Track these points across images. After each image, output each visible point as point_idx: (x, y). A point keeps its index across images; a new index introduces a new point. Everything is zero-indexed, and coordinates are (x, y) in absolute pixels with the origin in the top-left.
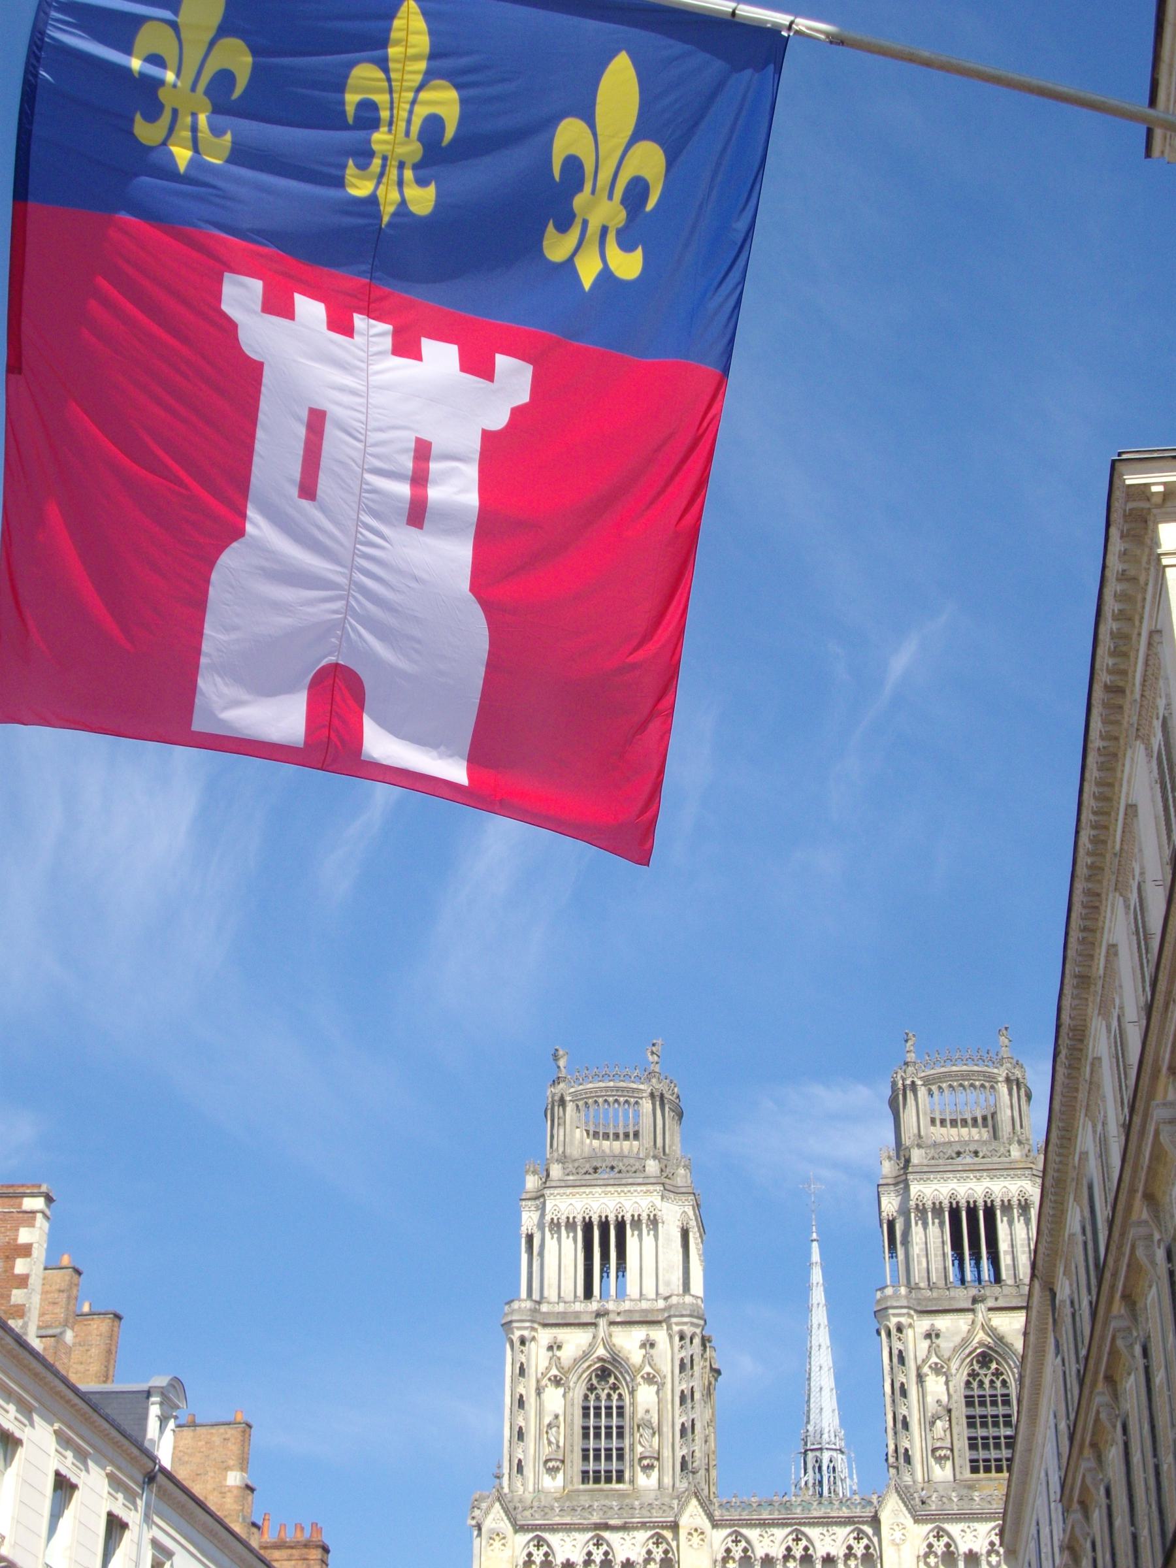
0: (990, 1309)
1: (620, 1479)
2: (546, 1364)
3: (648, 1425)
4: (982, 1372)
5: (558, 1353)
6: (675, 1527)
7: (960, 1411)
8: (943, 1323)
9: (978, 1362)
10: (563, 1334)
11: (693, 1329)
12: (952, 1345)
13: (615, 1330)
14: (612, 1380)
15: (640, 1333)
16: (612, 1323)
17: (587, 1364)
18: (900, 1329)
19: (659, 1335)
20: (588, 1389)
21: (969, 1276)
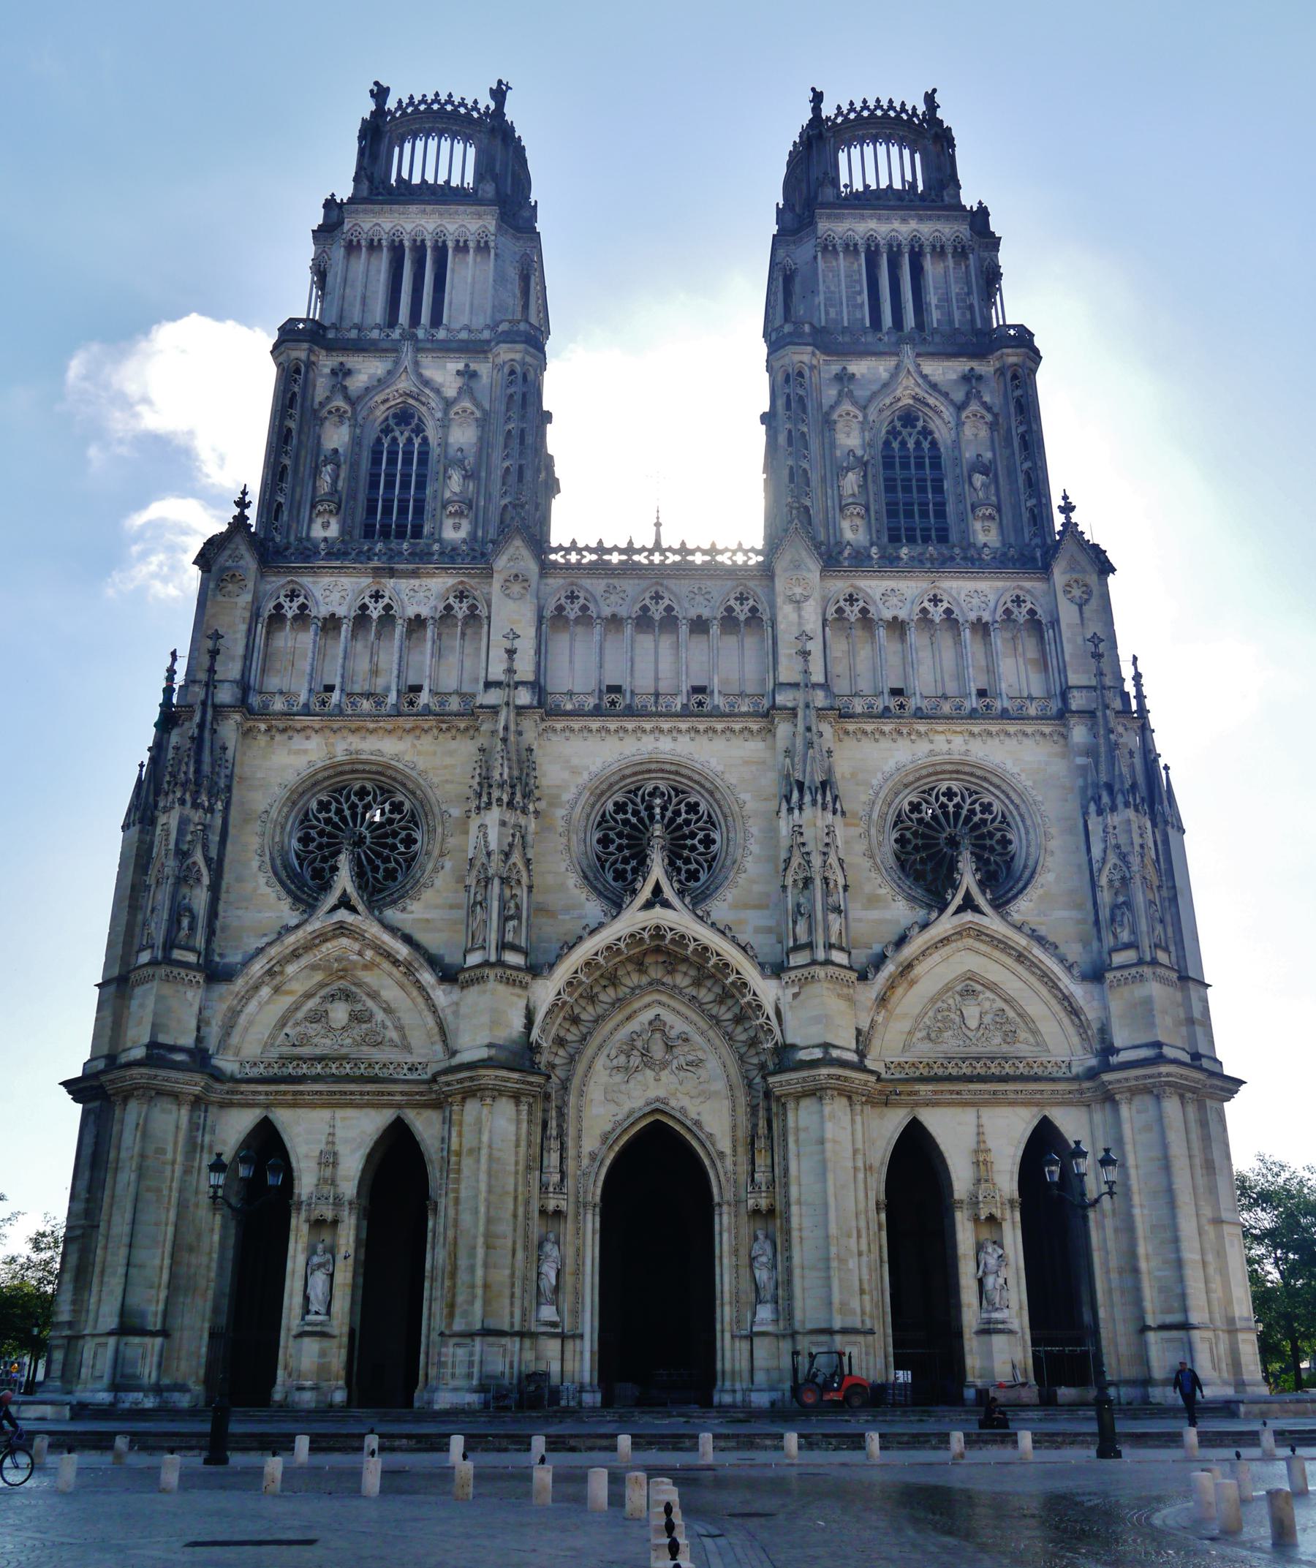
0: (918, 355)
1: (417, 533)
2: (328, 394)
3: (460, 463)
4: (905, 432)
5: (348, 382)
6: (489, 573)
7: (877, 470)
8: (859, 367)
9: (900, 418)
10: (352, 361)
11: (528, 359)
12: (868, 393)
13: (426, 360)
14: (416, 420)
15: (455, 365)
16: (418, 350)
17: (379, 398)
18: (800, 374)
19: (484, 369)
20: (382, 431)
21: (887, 320)
